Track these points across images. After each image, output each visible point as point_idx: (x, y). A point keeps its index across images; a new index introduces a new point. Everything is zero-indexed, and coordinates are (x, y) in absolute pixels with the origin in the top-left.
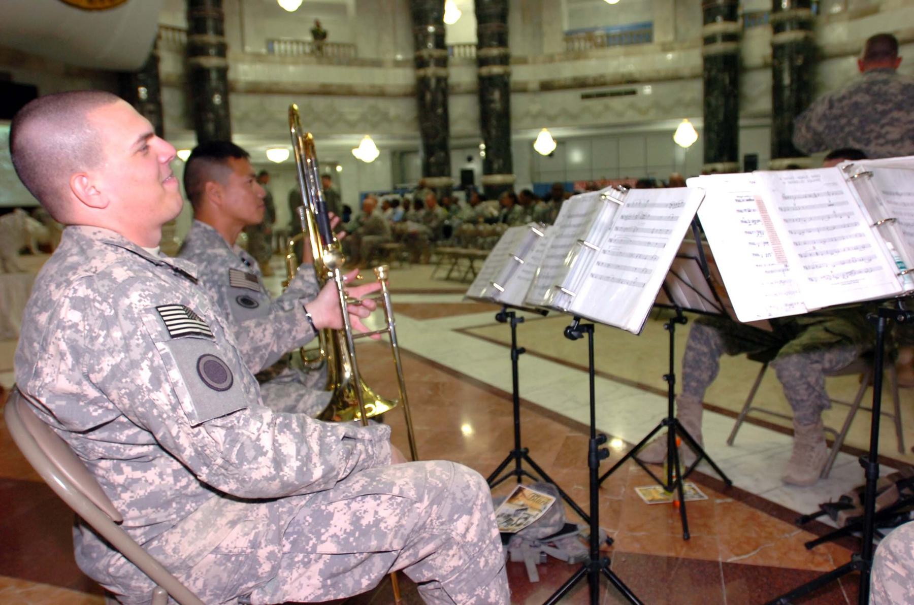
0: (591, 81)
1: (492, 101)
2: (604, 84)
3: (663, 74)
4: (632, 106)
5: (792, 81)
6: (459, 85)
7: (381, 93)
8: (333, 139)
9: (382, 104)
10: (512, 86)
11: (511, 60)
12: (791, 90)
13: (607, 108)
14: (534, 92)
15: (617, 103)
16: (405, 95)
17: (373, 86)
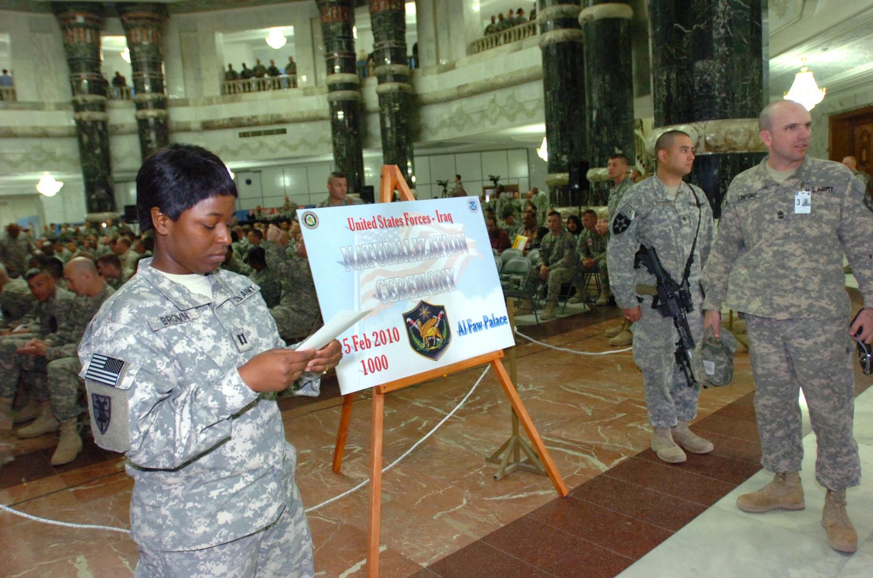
0: (245, 121)
1: (150, 142)
2: (257, 124)
3: (306, 115)
4: (283, 143)
5: (392, 125)
6: (122, 126)
7: (44, 134)
8: (16, 175)
9: (46, 144)
10: (173, 126)
11: (169, 103)
12: (392, 132)
13: (262, 144)
14: (197, 131)
15: (270, 140)
16: (70, 136)
17: (35, 128)
